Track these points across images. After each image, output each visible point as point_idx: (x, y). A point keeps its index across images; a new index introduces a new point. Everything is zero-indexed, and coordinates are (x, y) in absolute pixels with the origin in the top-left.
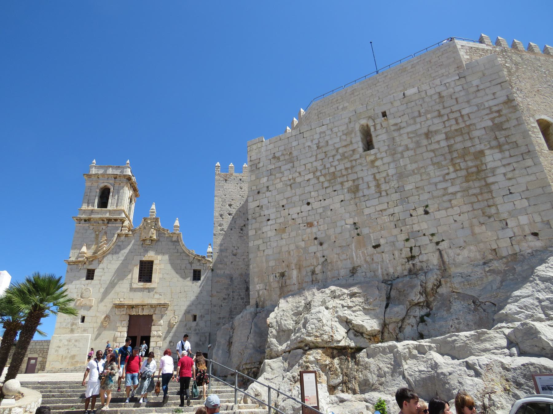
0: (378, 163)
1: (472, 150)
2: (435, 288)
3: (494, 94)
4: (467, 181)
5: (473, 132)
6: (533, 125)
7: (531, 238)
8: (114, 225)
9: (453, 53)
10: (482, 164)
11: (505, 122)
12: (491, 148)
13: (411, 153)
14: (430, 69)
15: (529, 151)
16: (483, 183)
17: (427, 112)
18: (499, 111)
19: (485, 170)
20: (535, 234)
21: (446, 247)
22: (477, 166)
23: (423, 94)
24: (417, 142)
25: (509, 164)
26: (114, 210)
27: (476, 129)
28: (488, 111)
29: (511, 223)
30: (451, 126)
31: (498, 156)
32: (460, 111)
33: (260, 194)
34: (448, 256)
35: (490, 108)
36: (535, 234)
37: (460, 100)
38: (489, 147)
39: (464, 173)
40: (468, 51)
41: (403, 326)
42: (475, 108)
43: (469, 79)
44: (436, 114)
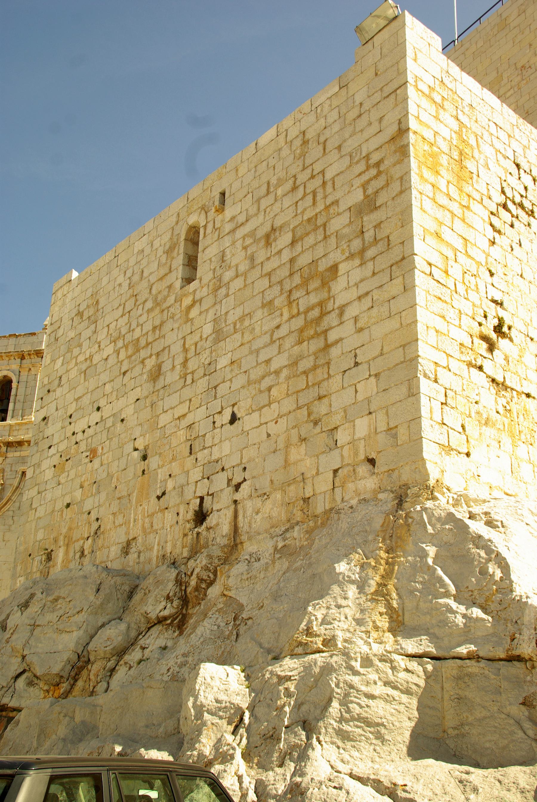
0: (194, 313)
1: (323, 266)
2: (203, 586)
3: (381, 120)
4: (300, 342)
5: (333, 221)
7: (363, 469)
8: (17, 454)
10: (329, 298)
11: (382, 188)
12: (352, 256)
13: (238, 283)
15: (403, 258)
16: (321, 343)
17: (280, 182)
18: (378, 164)
20: (372, 462)
21: (246, 497)
22: (321, 304)
23: (282, 138)
24: (252, 259)
25: (367, 294)
26: (19, 424)
27: (339, 214)
28: (361, 167)
29: (342, 437)
30: (303, 212)
31: (356, 275)
32: (323, 172)
33: (51, 393)
34: (244, 516)
35: (367, 157)
36: (372, 462)
37: (330, 146)
38: (347, 254)
39: (299, 322)
41: (117, 668)
42: (346, 161)
43: (353, 88)
44: (289, 185)
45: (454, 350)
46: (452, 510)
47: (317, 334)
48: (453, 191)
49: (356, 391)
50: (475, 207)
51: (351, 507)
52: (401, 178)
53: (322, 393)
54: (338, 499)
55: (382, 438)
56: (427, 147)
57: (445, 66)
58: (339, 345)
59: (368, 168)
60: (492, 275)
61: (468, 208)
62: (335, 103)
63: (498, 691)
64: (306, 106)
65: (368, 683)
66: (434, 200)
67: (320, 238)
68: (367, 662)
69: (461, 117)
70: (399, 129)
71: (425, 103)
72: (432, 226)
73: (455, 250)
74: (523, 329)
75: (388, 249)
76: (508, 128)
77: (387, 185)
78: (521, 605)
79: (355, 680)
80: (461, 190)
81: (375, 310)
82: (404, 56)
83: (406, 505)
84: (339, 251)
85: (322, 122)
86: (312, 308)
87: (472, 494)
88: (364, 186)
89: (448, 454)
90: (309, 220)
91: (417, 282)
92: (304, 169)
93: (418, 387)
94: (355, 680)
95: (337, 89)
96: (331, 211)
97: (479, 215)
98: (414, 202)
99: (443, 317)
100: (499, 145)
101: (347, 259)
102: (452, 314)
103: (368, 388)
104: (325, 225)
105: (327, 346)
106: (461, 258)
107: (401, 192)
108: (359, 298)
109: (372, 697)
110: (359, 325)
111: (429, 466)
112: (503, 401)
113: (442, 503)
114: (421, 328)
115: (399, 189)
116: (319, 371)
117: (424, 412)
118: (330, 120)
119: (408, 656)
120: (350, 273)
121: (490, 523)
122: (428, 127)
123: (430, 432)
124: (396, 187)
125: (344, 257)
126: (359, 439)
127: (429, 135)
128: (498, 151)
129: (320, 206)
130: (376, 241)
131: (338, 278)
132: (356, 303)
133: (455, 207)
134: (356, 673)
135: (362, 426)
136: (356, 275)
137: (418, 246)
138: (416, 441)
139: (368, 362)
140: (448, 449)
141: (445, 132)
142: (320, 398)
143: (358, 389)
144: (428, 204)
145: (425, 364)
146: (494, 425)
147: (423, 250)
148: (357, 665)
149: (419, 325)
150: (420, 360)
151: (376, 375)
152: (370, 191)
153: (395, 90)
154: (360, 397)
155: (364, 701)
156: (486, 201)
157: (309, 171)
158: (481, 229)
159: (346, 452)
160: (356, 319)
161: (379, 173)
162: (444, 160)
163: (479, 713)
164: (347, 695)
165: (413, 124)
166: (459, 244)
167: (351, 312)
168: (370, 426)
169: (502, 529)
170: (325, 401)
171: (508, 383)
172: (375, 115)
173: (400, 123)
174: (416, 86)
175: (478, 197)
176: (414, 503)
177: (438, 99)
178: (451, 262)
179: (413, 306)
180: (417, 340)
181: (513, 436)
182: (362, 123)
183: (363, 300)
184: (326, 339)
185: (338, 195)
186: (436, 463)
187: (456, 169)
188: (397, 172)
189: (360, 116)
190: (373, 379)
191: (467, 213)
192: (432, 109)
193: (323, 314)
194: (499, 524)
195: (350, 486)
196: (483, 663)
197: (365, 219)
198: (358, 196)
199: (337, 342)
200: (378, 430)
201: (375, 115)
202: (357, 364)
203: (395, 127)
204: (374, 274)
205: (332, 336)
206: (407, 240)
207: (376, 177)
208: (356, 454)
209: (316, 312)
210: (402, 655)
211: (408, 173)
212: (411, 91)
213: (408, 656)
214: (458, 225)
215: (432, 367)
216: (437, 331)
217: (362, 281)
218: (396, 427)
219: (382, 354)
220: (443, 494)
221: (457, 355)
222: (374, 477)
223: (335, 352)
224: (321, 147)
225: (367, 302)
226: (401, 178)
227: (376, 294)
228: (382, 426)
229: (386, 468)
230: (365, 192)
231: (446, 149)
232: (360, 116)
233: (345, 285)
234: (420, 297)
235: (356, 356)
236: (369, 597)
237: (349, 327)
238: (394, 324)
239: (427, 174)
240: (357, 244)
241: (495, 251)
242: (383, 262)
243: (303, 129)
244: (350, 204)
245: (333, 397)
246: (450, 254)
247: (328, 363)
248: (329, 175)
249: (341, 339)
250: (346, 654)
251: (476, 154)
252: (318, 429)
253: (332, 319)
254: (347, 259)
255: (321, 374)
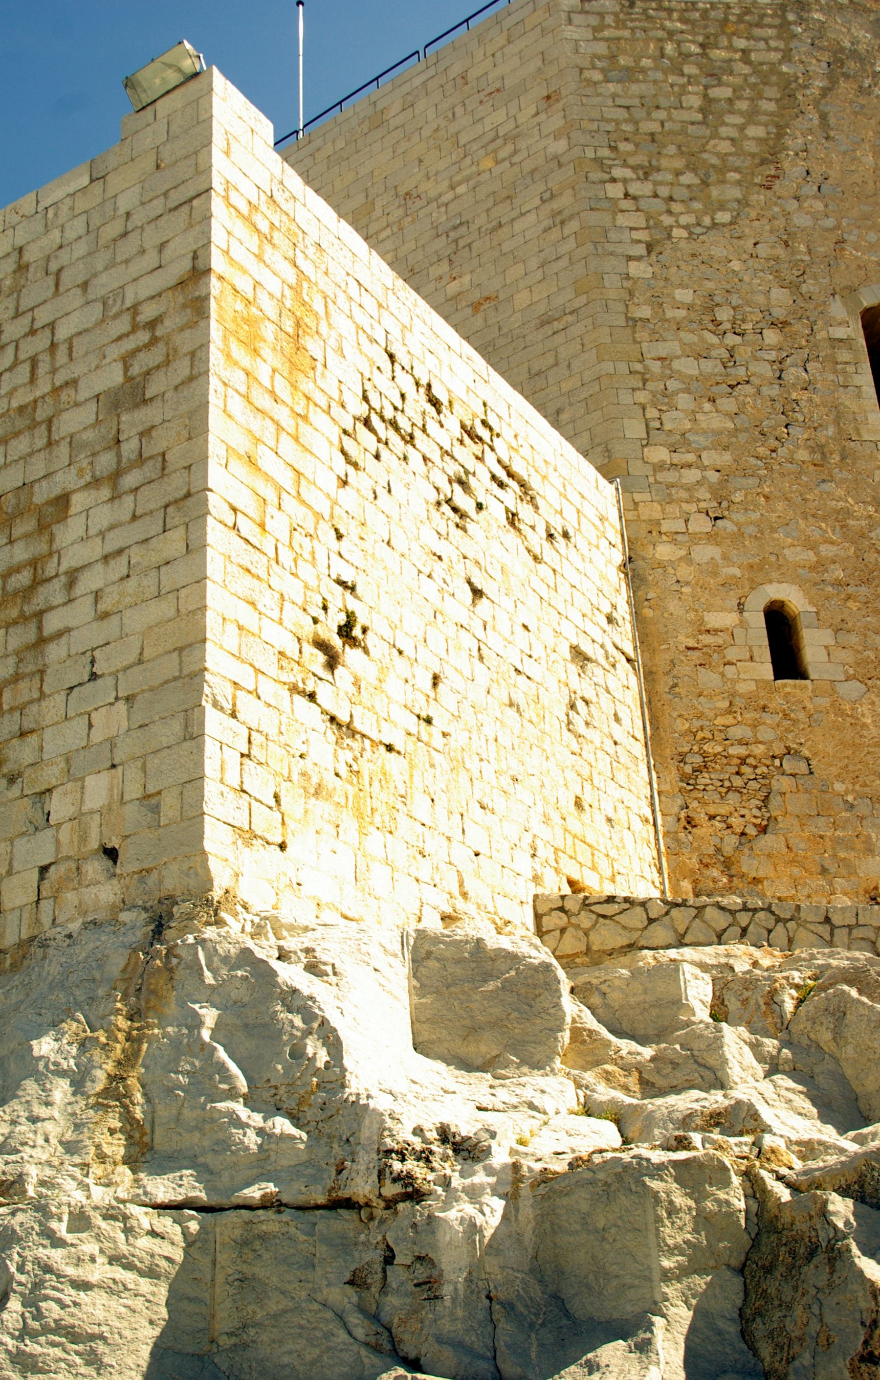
1: (42, 494)
3: (162, 247)
5: (65, 416)
6: (839, 333)
7: (95, 868)
9: (543, 33)
10: (51, 554)
11: (158, 367)
12: (96, 483)
14: (459, 110)
15: (188, 495)
16: (29, 634)
18: (152, 325)
19: (52, 578)
20: (112, 854)
22: (34, 563)
25: (120, 552)
27: (77, 405)
28: (123, 325)
29: (60, 807)
32: (52, 326)
35: (134, 309)
36: (112, 854)
37: (67, 279)
38: (88, 478)
40: (609, 20)
43: (114, 182)
45: (268, 662)
46: (250, 944)
47: (23, 618)
48: (282, 388)
49: (90, 726)
50: (317, 417)
51: (70, 936)
52: (193, 354)
53: (27, 725)
54: (46, 920)
55: (131, 811)
56: (239, 306)
57: (278, 173)
58: (64, 640)
59: (135, 328)
60: (339, 537)
61: (305, 418)
62: (82, 204)
63: (310, 1264)
64: (27, 203)
65: (79, 1261)
66: (247, 398)
67: (41, 443)
68: (80, 1221)
69: (300, 261)
70: (194, 267)
71: (240, 229)
72: (242, 444)
73: (280, 489)
74: (388, 634)
75: (163, 476)
76: (378, 291)
77: (167, 362)
78: (358, 1110)
79: (56, 1256)
80: (294, 386)
81: (132, 583)
82: (207, 143)
83: (168, 934)
84: (73, 470)
85: (56, 234)
86: (18, 569)
87: (286, 916)
88: (126, 360)
89: (248, 844)
90: (21, 409)
91: (210, 539)
92: (17, 315)
93: (202, 724)
94: (56, 1256)
95: (86, 180)
96: (64, 397)
97: (323, 434)
98: (212, 397)
99: (253, 604)
100: (362, 319)
101: (88, 486)
102: (267, 600)
103: (111, 721)
104: (50, 421)
105: (42, 641)
106: (289, 502)
107: (191, 379)
108: (106, 558)
109: (84, 1286)
110: (102, 607)
111: (214, 865)
112: (346, 756)
113: (234, 932)
114: (212, 620)
115: (187, 372)
116: (23, 685)
117: (210, 768)
118: (70, 235)
119: (156, 1206)
120: (91, 512)
121: (313, 968)
122: (245, 271)
123: (219, 805)
124: (182, 368)
125: (82, 482)
126: (92, 813)
127: (245, 285)
128: (359, 328)
129: (44, 387)
130: (141, 459)
131: (69, 520)
132: (99, 567)
133: (282, 414)
134: (57, 1242)
135: (98, 789)
136: (103, 516)
137: (216, 476)
138: (194, 819)
139: (115, 674)
140: (248, 836)
141: (273, 285)
142: (23, 734)
143: (94, 722)
144: (236, 405)
145: (216, 684)
146: (330, 796)
147: (224, 483)
148: (60, 1228)
149: (209, 614)
150: (208, 676)
151: (128, 699)
152: (135, 370)
153: (188, 198)
154: (97, 736)
155: (69, 1294)
156: (336, 410)
157: (26, 320)
158: (325, 458)
159: (64, 835)
160: (97, 596)
161: (154, 341)
162: (268, 331)
163: (274, 1305)
164: (38, 1285)
165: (217, 262)
166: (286, 479)
167: (89, 582)
168: (111, 790)
169: (333, 979)
170: (32, 739)
171: (357, 725)
172: (152, 237)
173: (195, 257)
174: (226, 198)
175: (323, 401)
176: (184, 931)
177: (264, 227)
178: (271, 510)
179: (201, 580)
180: (204, 640)
181: (360, 817)
182: (127, 248)
183: (112, 563)
184: (40, 628)
185: (78, 370)
186: (227, 861)
187: (289, 348)
188: (185, 342)
189: (125, 234)
190: (122, 706)
191: (303, 427)
192: (253, 242)
193: (37, 582)
194: (329, 969)
195: (70, 897)
196: (287, 1215)
197: (124, 418)
198: (114, 376)
199: (59, 634)
200: (127, 798)
201: (152, 237)
202: (94, 677)
203: (186, 264)
204: (134, 517)
205: (52, 623)
206: (198, 463)
207: (148, 346)
208: (84, 839)
209: (24, 578)
210: (146, 1206)
211: (205, 346)
212: (217, 205)
213: (156, 1206)
214: (286, 445)
215: (229, 690)
216: (240, 628)
217: (112, 528)
218: (159, 793)
219: (140, 662)
220: (236, 915)
221: (272, 670)
222: (115, 881)
223: (55, 652)
224: (51, 281)
225: (119, 567)
226: (193, 354)
227: (136, 555)
228: (134, 791)
229: (136, 866)
230: (126, 369)
231: (272, 314)
232: (125, 234)
233: (82, 532)
234: (214, 565)
235: (93, 662)
236: (92, 1101)
237: (83, 609)
238: (164, 609)
239: (238, 352)
240: (106, 462)
241: (345, 496)
242: (151, 498)
243: (19, 242)
244: (98, 389)
245: (48, 734)
246: (270, 495)
247: (42, 672)
248: (63, 332)
249: (68, 630)
250: (41, 1208)
251: (323, 328)
252: (15, 791)
253: (54, 592)
254: (88, 486)
255: (26, 690)
